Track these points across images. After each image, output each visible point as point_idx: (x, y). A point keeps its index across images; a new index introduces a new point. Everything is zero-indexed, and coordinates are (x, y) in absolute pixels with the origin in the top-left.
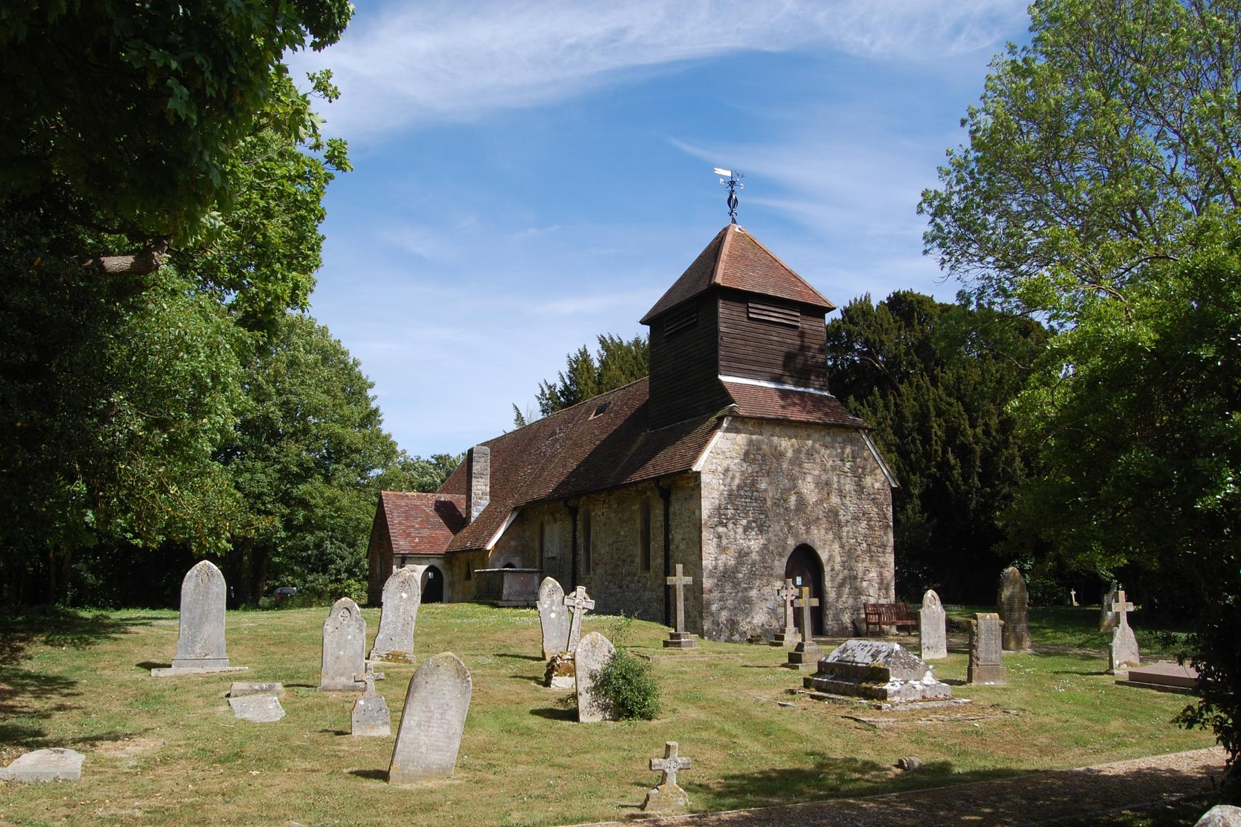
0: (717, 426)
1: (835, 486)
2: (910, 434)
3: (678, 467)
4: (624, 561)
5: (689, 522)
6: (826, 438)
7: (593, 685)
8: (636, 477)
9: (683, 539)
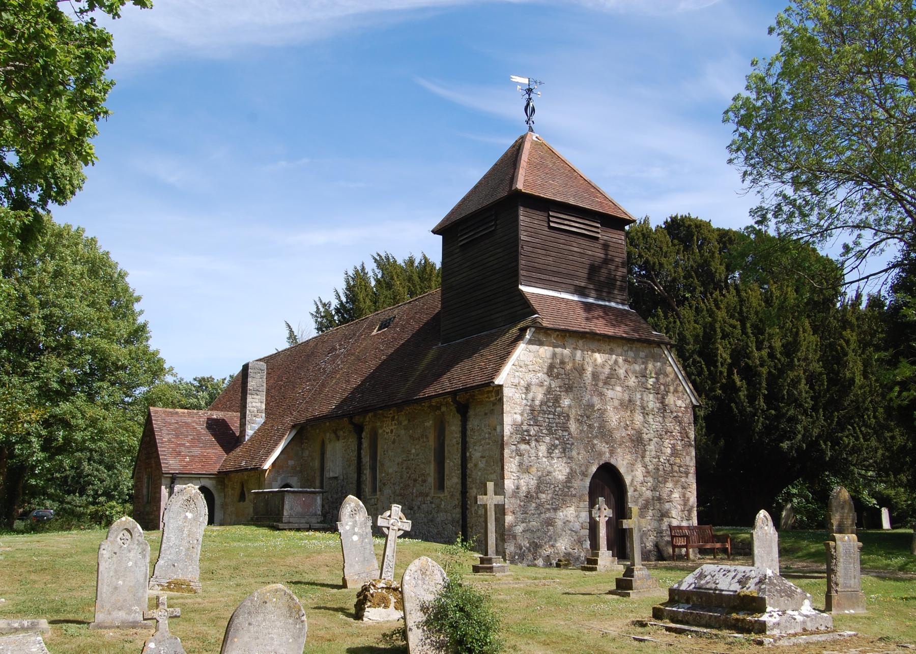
0: (520, 337)
1: (638, 403)
2: (691, 356)
3: (479, 380)
4: (415, 480)
5: (489, 438)
6: (629, 352)
7: (424, 619)
8: (430, 391)
9: (482, 457)
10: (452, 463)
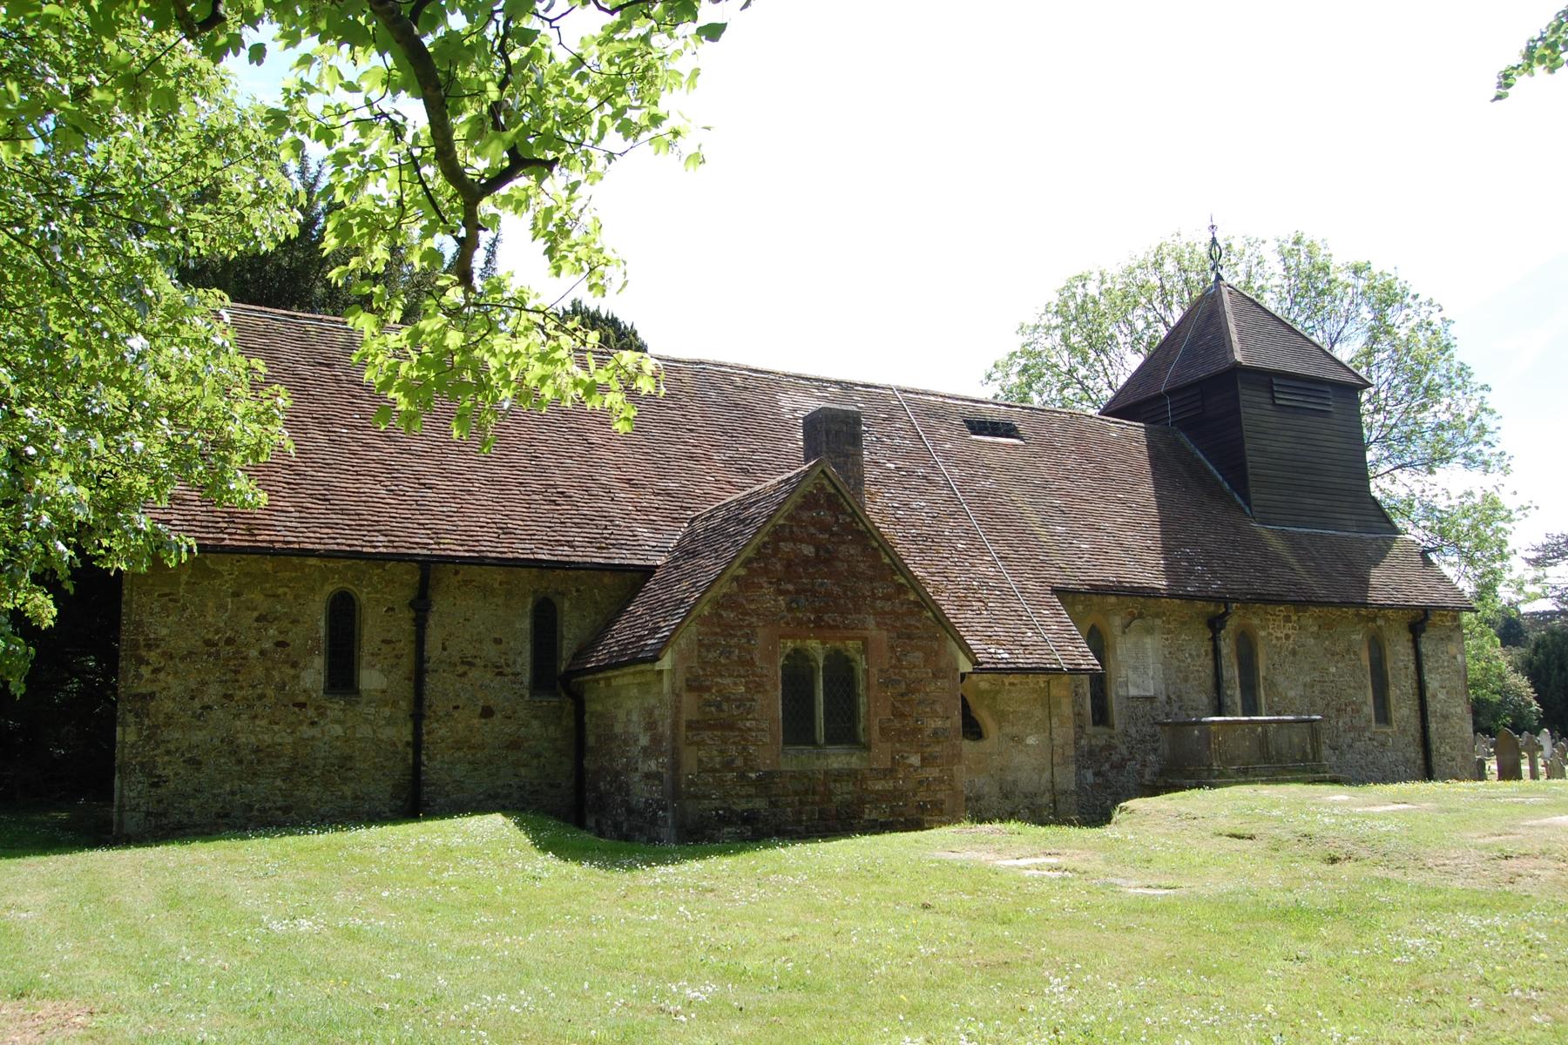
10: (1398, 692)
